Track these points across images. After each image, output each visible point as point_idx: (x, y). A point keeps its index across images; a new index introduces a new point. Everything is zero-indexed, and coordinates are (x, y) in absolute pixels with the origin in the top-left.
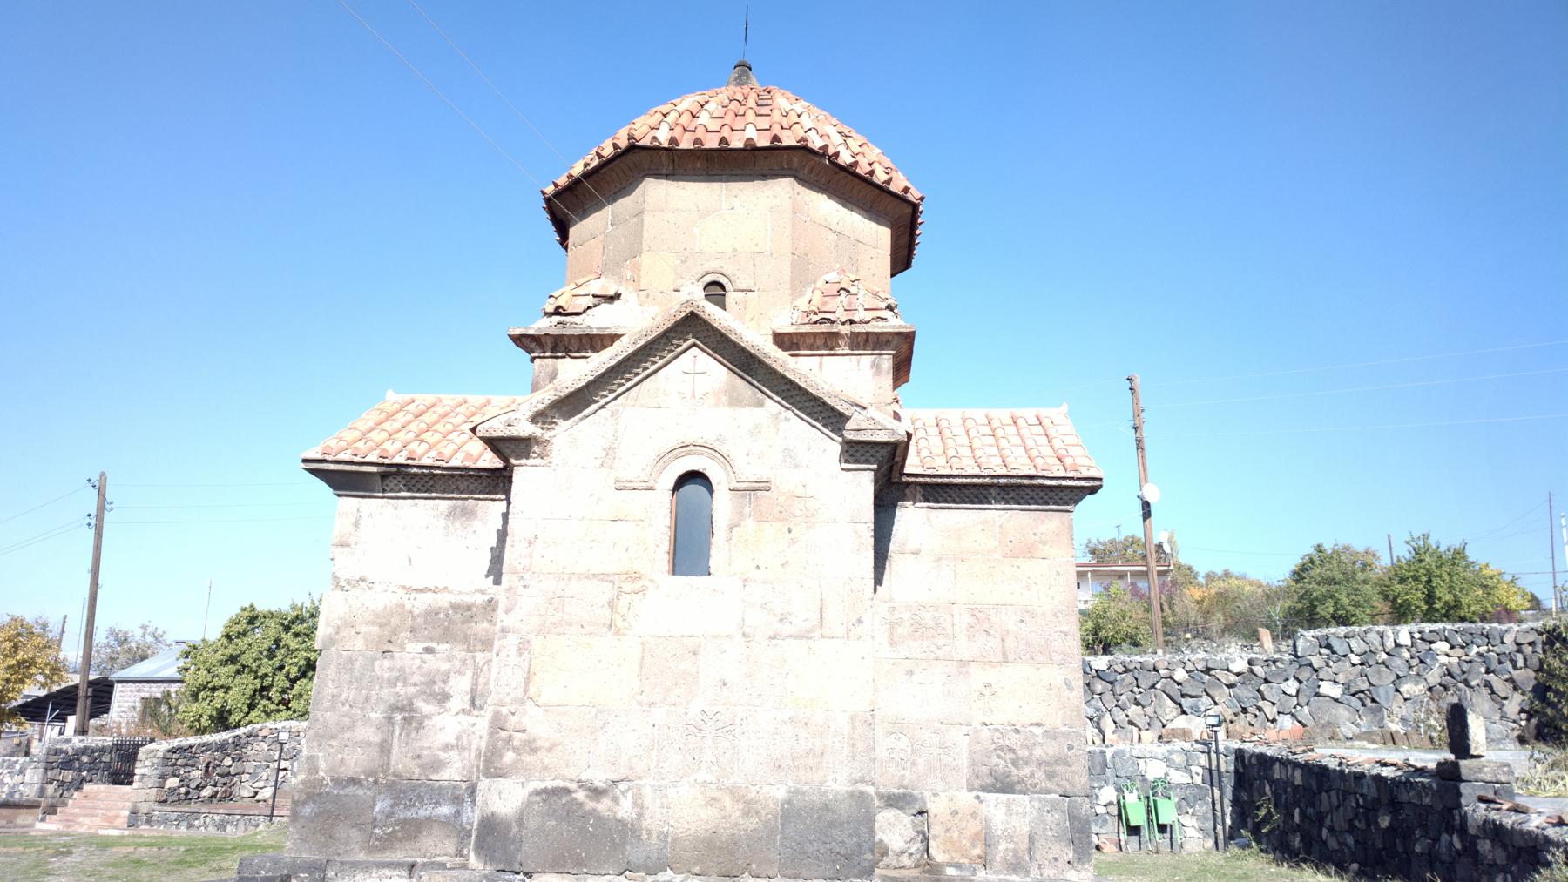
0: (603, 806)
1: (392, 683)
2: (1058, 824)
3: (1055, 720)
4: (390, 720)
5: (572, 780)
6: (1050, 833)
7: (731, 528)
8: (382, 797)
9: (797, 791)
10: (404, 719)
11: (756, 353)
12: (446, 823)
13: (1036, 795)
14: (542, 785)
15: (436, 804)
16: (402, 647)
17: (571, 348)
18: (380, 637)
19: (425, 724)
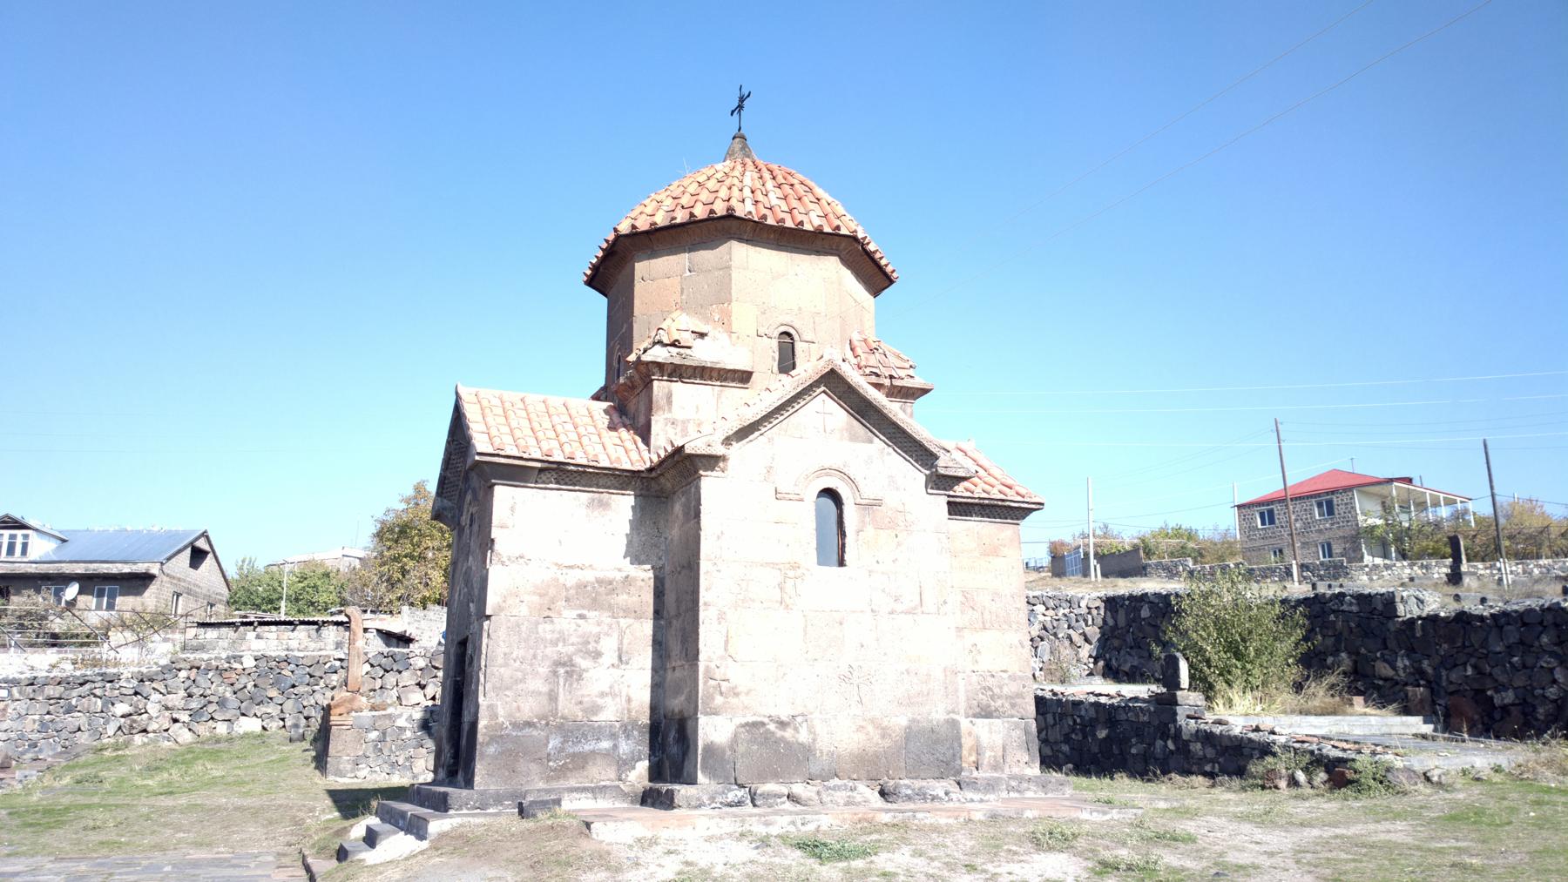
0: (788, 734)
1: (555, 643)
2: (1019, 738)
3: (1014, 669)
4: (555, 673)
5: (765, 716)
6: (1015, 744)
7: (858, 532)
8: (554, 736)
9: (913, 721)
10: (567, 672)
11: (877, 405)
12: (607, 755)
13: (1006, 719)
14: (744, 721)
15: (597, 740)
16: (560, 614)
17: (685, 375)
18: (541, 605)
19: (583, 676)
